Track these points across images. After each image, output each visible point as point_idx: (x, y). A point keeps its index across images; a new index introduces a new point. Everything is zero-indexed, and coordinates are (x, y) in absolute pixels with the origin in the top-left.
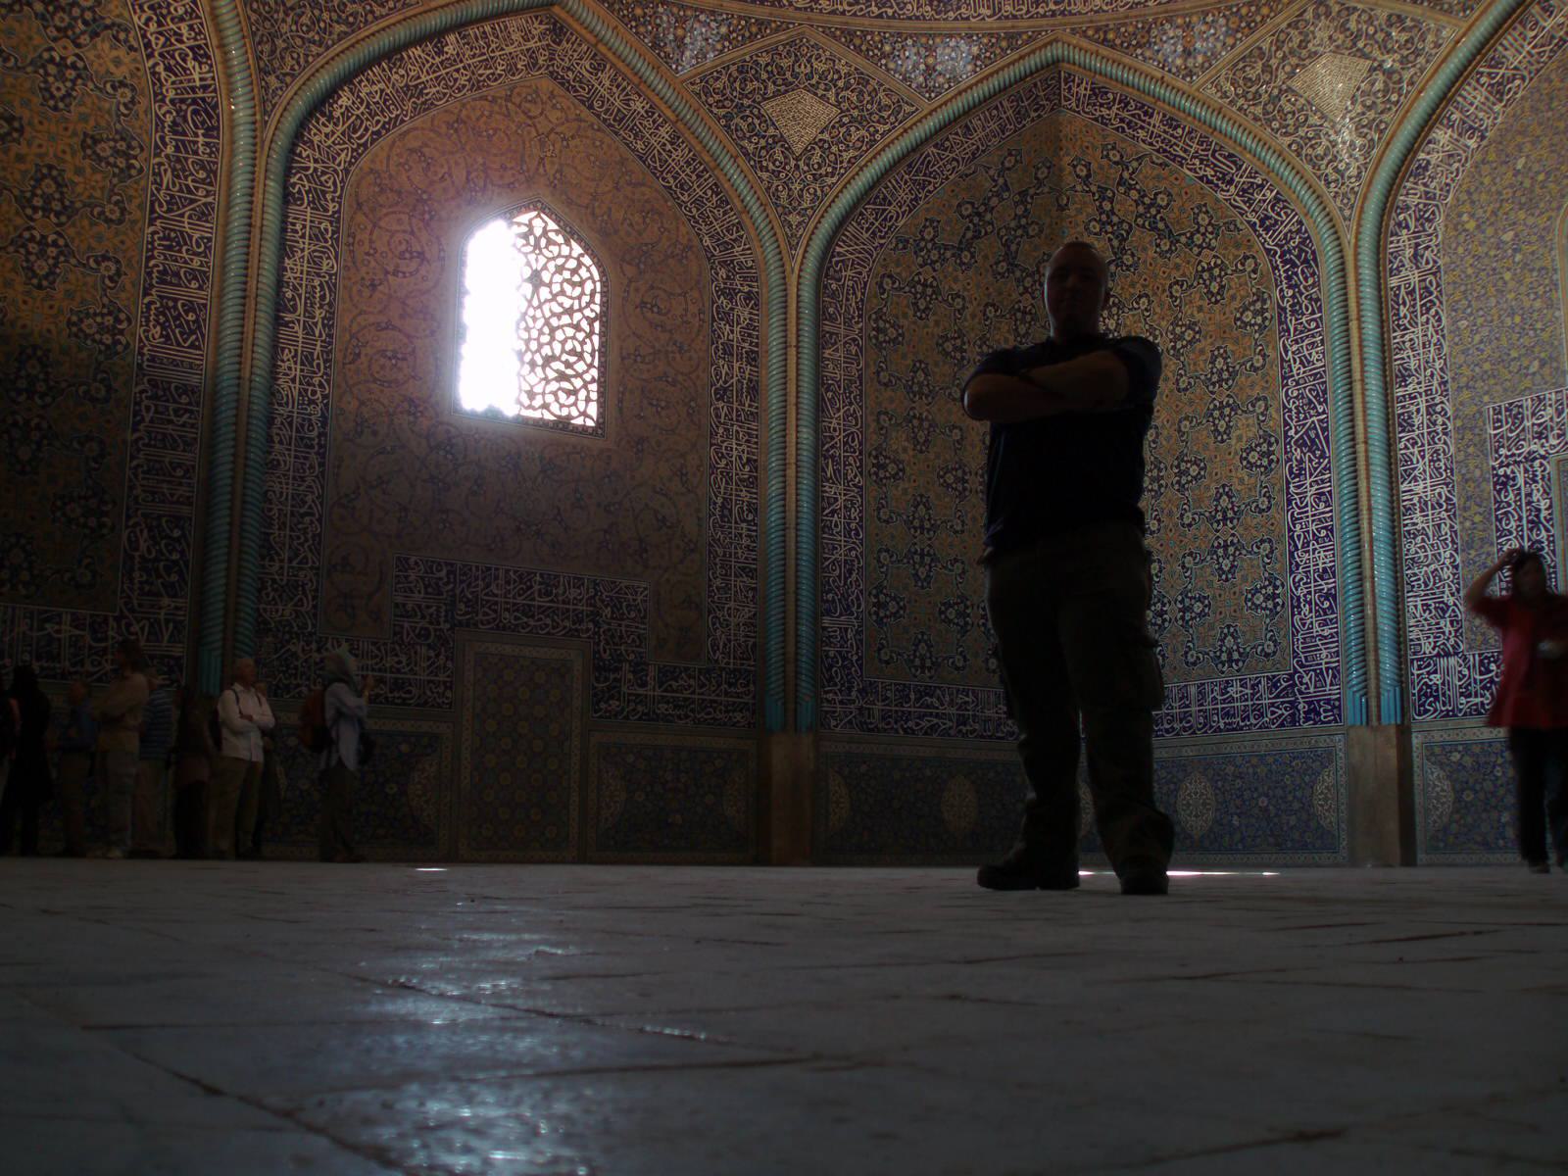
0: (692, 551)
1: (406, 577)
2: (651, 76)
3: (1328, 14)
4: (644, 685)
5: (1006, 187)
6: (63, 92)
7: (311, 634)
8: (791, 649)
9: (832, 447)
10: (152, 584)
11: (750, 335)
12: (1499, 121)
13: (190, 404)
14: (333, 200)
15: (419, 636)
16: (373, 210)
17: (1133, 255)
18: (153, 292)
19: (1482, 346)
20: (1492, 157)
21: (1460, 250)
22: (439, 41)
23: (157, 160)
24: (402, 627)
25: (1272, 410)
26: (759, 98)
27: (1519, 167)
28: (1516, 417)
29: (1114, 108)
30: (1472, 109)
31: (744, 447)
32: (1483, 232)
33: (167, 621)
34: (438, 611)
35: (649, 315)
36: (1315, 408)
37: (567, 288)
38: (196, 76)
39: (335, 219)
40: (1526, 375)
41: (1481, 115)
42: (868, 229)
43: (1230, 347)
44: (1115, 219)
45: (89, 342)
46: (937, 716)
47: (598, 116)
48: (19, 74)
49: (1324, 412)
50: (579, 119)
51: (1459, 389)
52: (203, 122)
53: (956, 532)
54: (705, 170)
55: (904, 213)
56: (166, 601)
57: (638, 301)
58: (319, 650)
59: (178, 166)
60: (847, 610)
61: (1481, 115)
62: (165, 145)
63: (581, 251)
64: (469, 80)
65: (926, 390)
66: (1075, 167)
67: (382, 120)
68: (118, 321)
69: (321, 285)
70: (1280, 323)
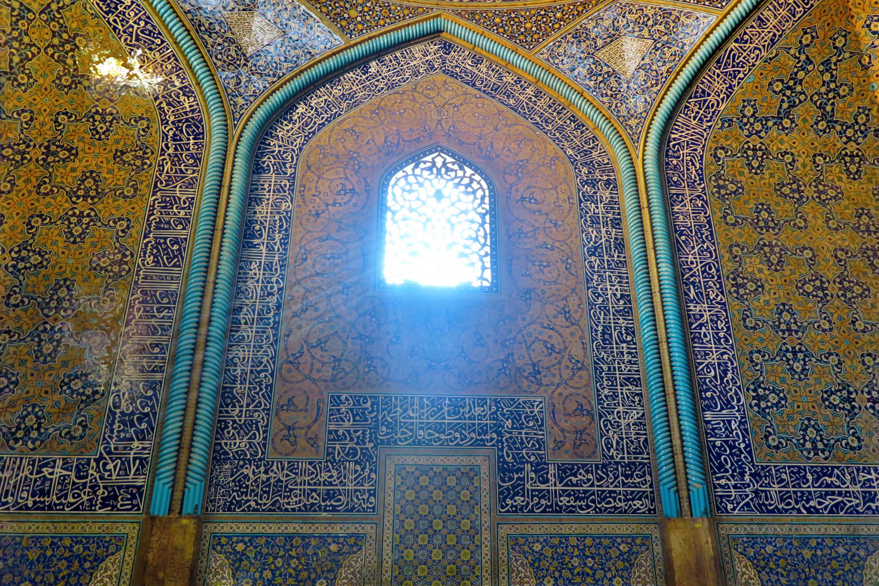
0: (580, 369)
1: (338, 410)
2: (511, 57)
4: (546, 481)
5: (809, 61)
6: (105, 129)
7: (260, 460)
8: (677, 442)
9: (692, 276)
10: (127, 432)
11: (612, 208)
13: (169, 303)
14: (290, 167)
15: (347, 455)
16: (318, 169)
18: (151, 235)
22: (365, 67)
23: (162, 157)
24: (334, 448)
26: (591, 51)
31: (617, 287)
33: (135, 459)
34: (364, 433)
35: (528, 205)
37: (463, 197)
38: (187, 105)
39: (293, 177)
42: (695, 118)
45: (103, 272)
46: (840, 494)
47: (480, 90)
48: (78, 123)
50: (465, 93)
52: (194, 131)
53: (824, 330)
54: (563, 108)
55: (723, 100)
56: (136, 444)
57: (519, 198)
58: (266, 472)
59: (176, 159)
60: (728, 404)
62: (168, 148)
63: (473, 172)
64: (386, 85)
65: (771, 224)
66: (868, 26)
67: (326, 116)
68: (125, 256)
69: (280, 219)
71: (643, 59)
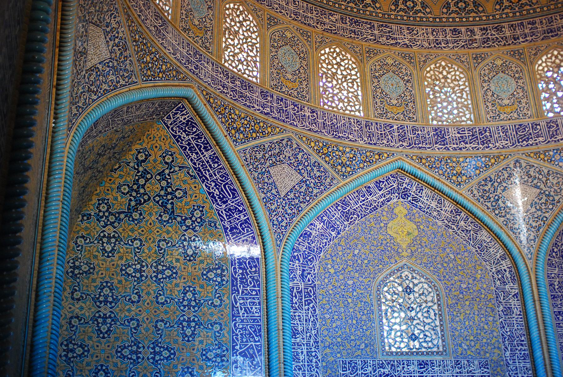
3: (291, 146)
12: (347, 229)
17: (141, 214)
19: (337, 329)
20: (343, 243)
21: (326, 280)
25: (225, 332)
27: (356, 253)
28: (353, 367)
29: (190, 137)
30: (334, 219)
36: (253, 337)
40: (359, 349)
41: (338, 223)
43: (198, 289)
44: (142, 191)
49: (259, 340)
51: (325, 347)
61: (338, 223)
66: (139, 152)
70: (233, 285)
71: (100, 63)
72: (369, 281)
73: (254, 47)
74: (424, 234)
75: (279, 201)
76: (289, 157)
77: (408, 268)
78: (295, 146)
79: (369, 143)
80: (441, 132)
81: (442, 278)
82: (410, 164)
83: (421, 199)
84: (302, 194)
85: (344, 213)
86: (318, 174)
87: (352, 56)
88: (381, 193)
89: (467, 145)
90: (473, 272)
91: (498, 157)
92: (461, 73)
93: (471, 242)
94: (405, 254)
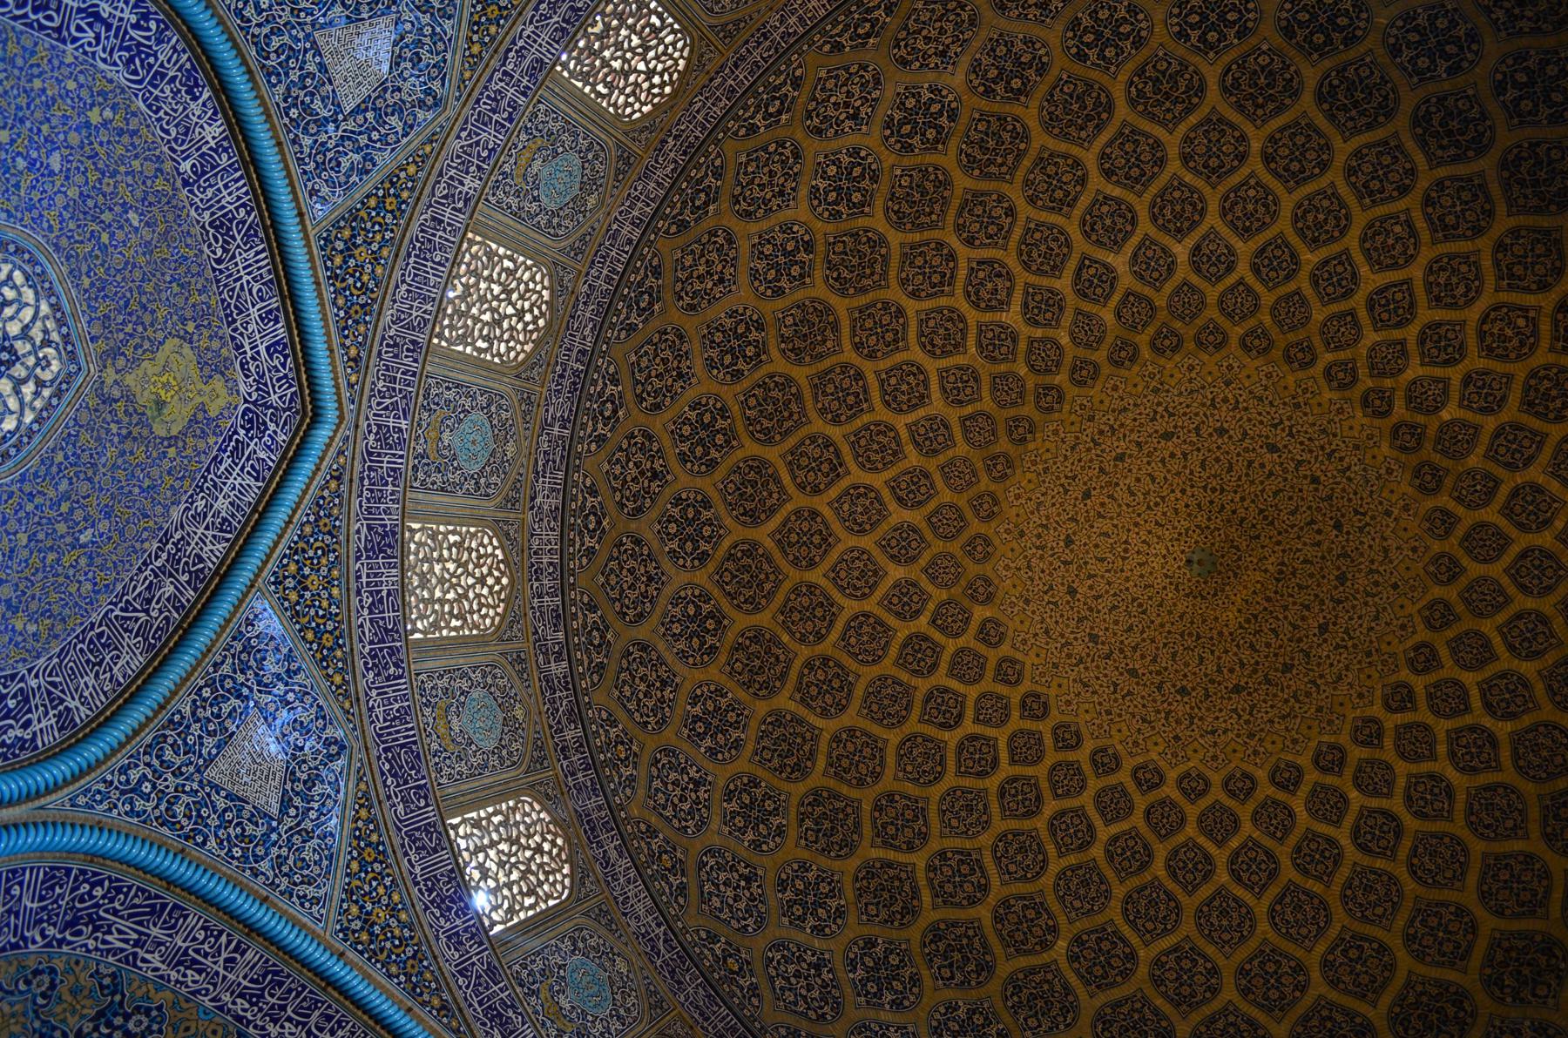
12: (193, 213)
21: (71, 85)
30: (221, 185)
32: (77, 129)
41: (210, 192)
61: (210, 192)
72: (50, 227)
73: (604, 91)
74: (155, 454)
75: (309, 19)
76: (399, 90)
77: (69, 374)
78: (421, 115)
79: (383, 338)
80: (390, 546)
81: (27, 488)
82: (328, 446)
83: (237, 469)
84: (308, 99)
85: (231, 221)
86: (345, 165)
87: (529, 356)
88: (263, 353)
89: (366, 612)
90: (34, 606)
91: (346, 696)
92: (493, 619)
93: (117, 612)
94: (110, 376)
